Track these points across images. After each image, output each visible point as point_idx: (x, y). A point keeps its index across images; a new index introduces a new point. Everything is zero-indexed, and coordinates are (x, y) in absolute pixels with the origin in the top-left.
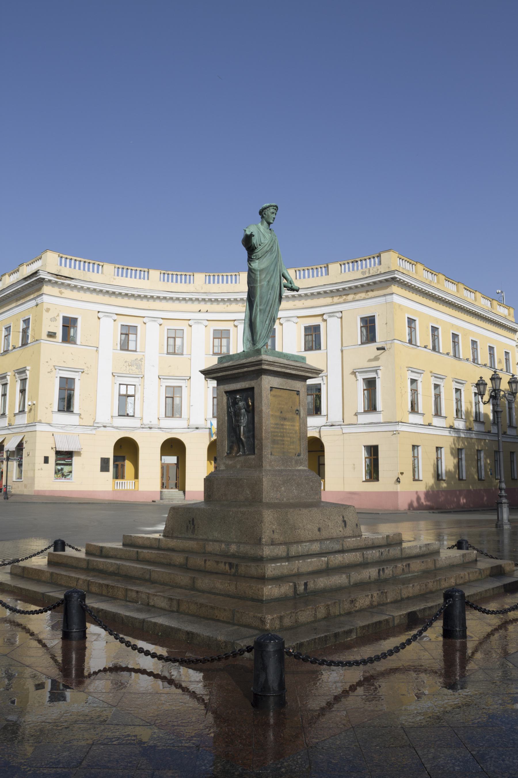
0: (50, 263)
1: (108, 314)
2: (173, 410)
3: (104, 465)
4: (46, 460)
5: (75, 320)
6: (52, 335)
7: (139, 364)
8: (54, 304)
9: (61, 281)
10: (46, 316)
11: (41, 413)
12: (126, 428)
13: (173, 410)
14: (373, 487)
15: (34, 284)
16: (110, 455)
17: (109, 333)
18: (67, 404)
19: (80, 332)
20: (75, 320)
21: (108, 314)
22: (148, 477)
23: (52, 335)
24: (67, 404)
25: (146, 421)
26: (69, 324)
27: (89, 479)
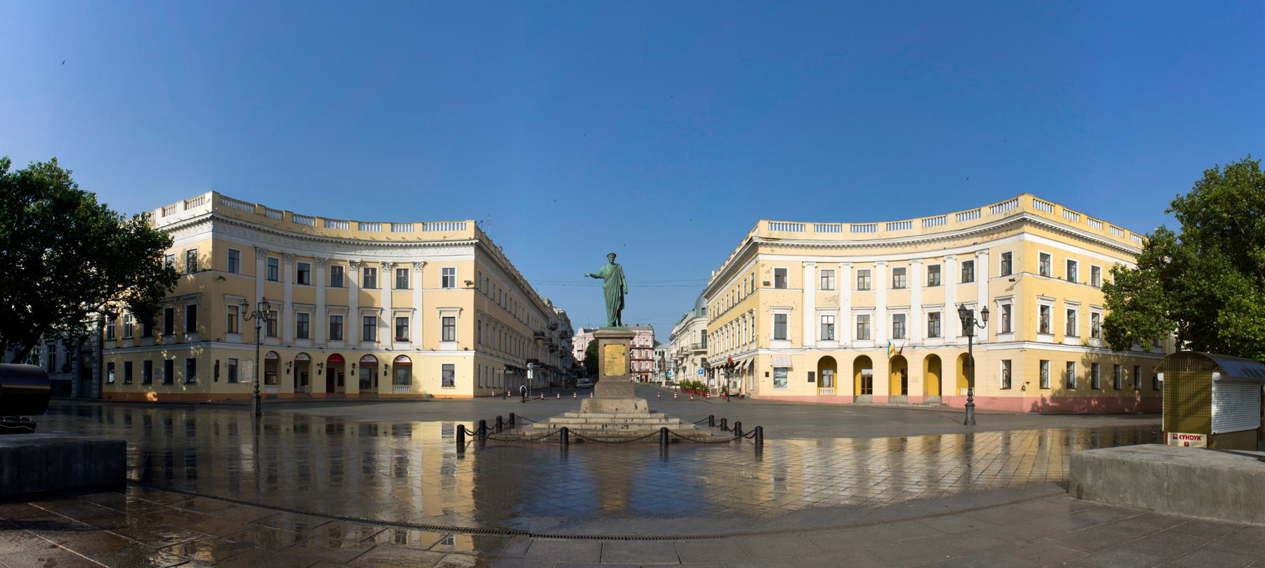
0: (763, 229)
1: (810, 263)
2: (863, 333)
3: (811, 377)
4: (767, 374)
5: (784, 271)
6: (767, 284)
7: (836, 299)
8: (768, 260)
9: (771, 242)
10: (762, 270)
11: (762, 342)
12: (827, 348)
13: (863, 333)
14: (1007, 393)
15: (753, 248)
16: (815, 369)
17: (811, 277)
18: (780, 335)
19: (789, 279)
20: (784, 271)
21: (810, 263)
22: (844, 385)
23: (767, 284)
24: (780, 335)
25: (842, 343)
26: (780, 275)
27: (799, 388)
